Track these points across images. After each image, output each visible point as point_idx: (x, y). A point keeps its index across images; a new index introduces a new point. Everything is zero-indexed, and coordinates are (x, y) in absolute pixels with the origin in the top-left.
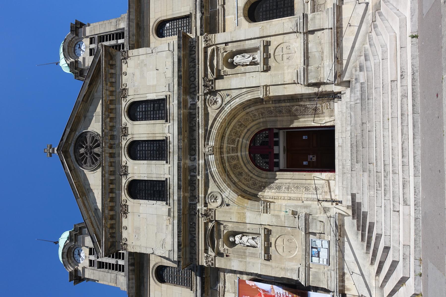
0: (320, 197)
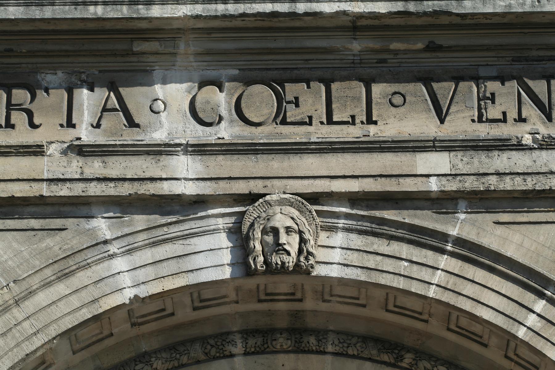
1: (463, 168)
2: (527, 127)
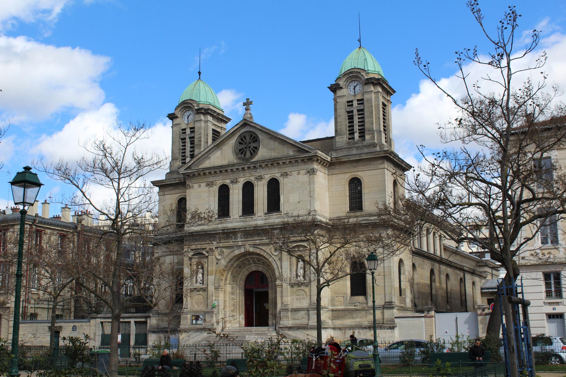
0: (227, 319)
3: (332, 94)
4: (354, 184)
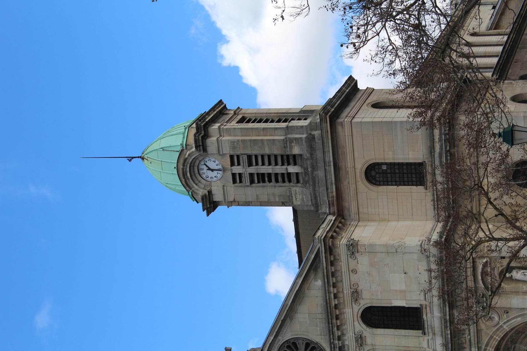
1: (474, 346)
2: (467, 337)
3: (219, 208)
4: (377, 175)
